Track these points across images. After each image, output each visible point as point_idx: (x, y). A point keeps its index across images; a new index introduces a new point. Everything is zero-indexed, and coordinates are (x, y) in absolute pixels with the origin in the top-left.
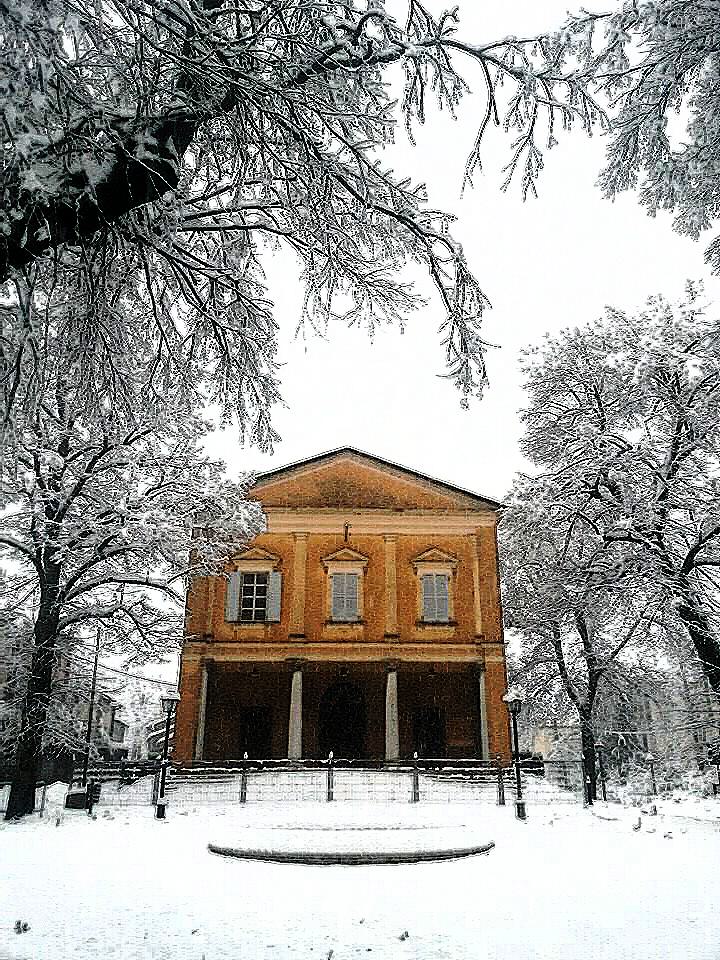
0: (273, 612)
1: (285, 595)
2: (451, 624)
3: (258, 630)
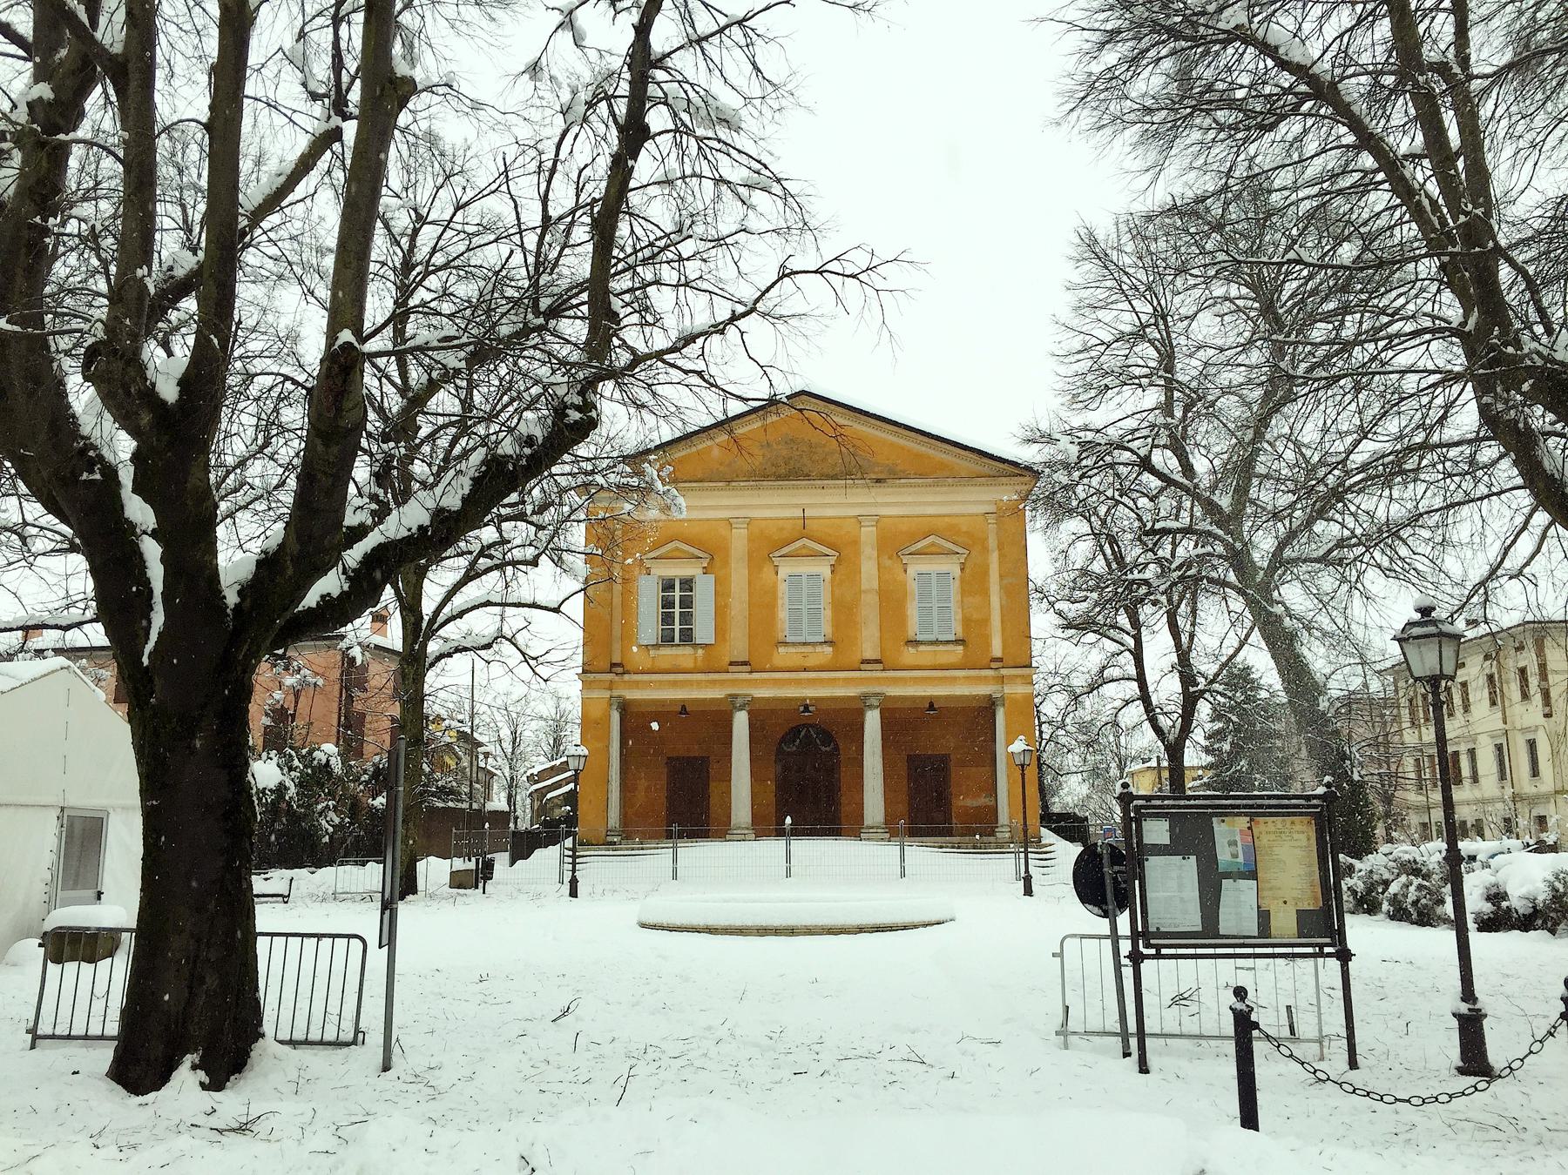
0: (704, 630)
1: (721, 612)
2: (957, 642)
3: (682, 655)
